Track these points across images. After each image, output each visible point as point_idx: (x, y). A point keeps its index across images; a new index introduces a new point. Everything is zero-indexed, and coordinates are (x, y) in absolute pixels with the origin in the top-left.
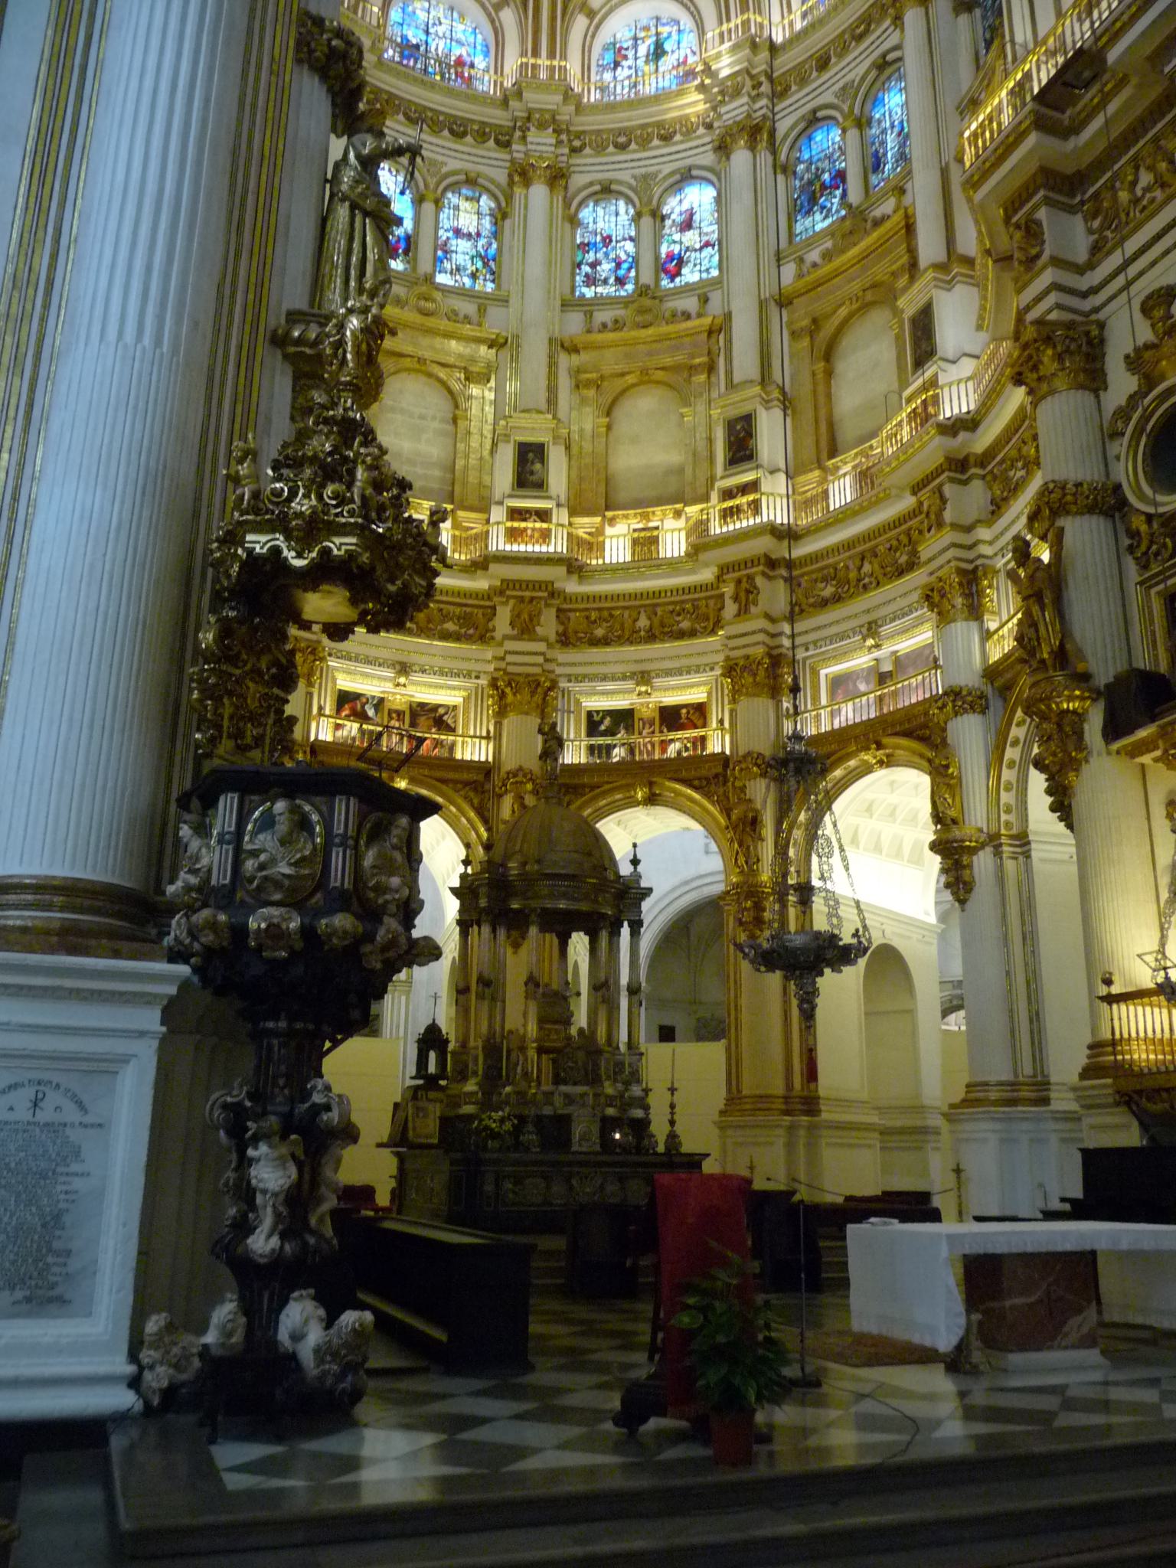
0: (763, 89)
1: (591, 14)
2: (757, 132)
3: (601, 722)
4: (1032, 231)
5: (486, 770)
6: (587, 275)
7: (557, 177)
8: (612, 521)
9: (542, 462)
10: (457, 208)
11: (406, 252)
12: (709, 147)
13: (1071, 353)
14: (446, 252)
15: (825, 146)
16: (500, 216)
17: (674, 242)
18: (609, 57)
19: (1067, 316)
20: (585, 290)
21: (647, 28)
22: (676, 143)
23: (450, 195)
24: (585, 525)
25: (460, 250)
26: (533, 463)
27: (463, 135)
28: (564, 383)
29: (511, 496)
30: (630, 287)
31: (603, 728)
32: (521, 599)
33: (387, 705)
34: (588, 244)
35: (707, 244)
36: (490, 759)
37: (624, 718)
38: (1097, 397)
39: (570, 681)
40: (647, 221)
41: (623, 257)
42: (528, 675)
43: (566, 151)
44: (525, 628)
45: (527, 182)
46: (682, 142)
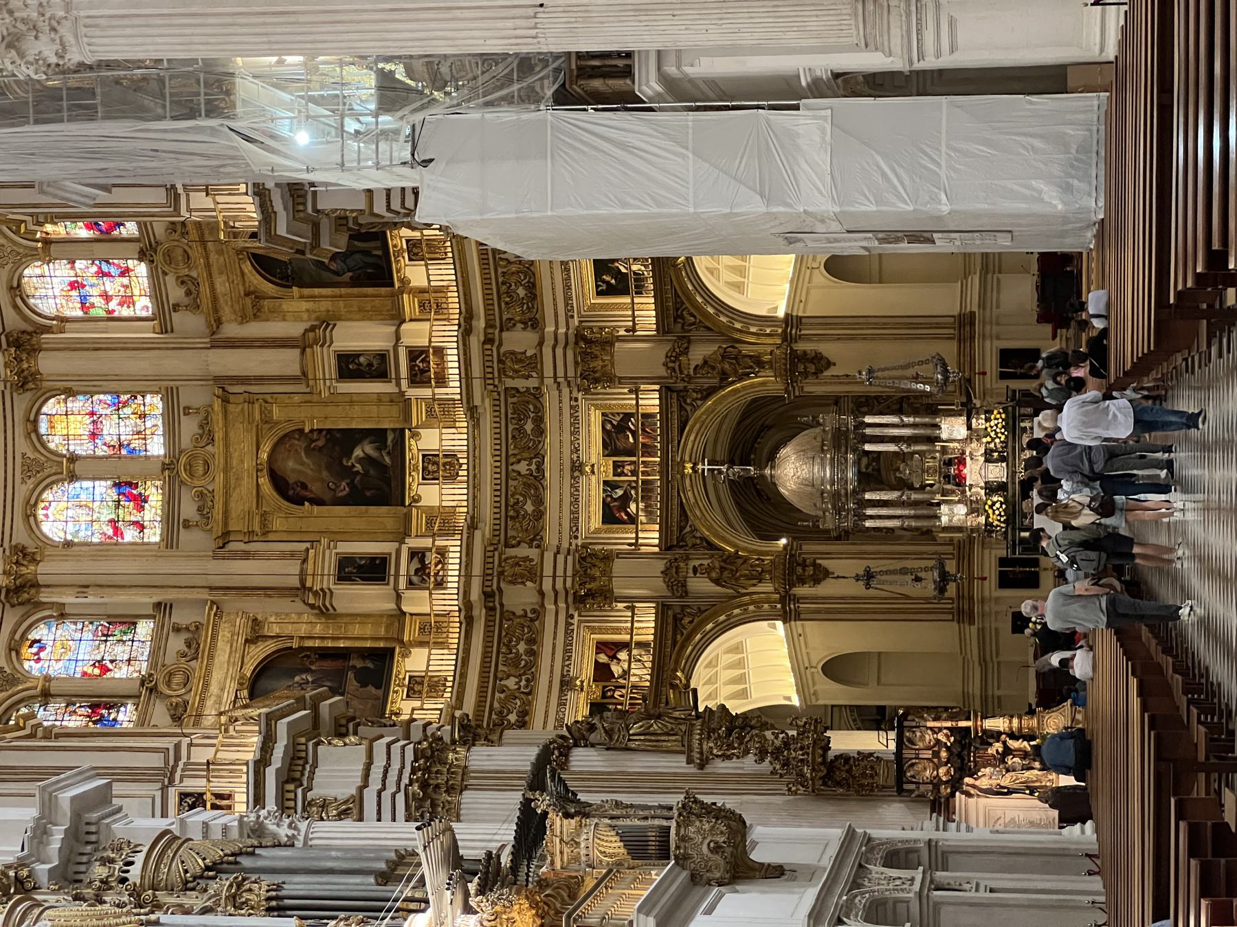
3: (608, 283)
5: (666, 392)
6: (121, 304)
8: (405, 282)
9: (359, 355)
16: (70, 393)
20: (138, 306)
23: (52, 446)
24: (409, 304)
25: (114, 431)
26: (360, 364)
28: (255, 329)
29: (398, 384)
30: (131, 263)
31: (613, 281)
32: (502, 372)
33: (611, 478)
36: (657, 387)
39: (572, 317)
41: (95, 269)
42: (576, 363)
44: (532, 364)
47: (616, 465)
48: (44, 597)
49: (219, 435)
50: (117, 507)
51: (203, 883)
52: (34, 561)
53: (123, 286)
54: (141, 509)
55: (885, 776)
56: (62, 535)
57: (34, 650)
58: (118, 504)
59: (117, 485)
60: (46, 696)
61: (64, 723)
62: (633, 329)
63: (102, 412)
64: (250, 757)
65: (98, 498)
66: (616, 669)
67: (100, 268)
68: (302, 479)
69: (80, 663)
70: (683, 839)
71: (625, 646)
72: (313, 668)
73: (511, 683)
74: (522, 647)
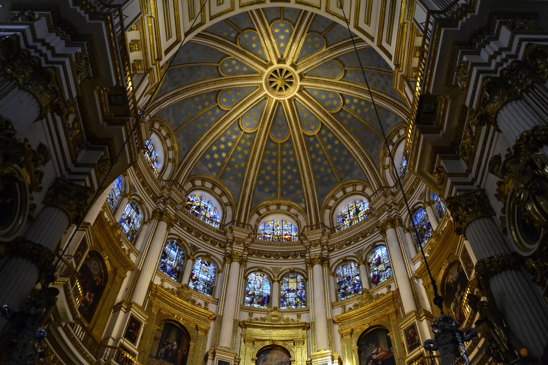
0: (393, 208)
1: (330, 208)
2: (393, 222)
4: (440, 170)
6: (343, 293)
7: (323, 261)
12: (379, 234)
13: (471, 206)
15: (421, 217)
16: (305, 281)
17: (375, 271)
18: (340, 219)
19: (462, 193)
20: (342, 299)
21: (352, 206)
22: (368, 237)
27: (288, 257)
28: (338, 336)
34: (342, 281)
35: (388, 267)
38: (492, 219)
40: (362, 267)
41: (356, 282)
43: (327, 251)
46: (370, 236)
48: (227, 265)
50: (259, 296)
53: (350, 292)
54: (258, 303)
56: (250, 279)
57: (206, 263)
58: (262, 296)
60: (186, 257)
61: (174, 261)
63: (298, 292)
65: (263, 291)
67: (357, 284)
68: (268, 360)
69: (198, 274)
72: (179, 351)
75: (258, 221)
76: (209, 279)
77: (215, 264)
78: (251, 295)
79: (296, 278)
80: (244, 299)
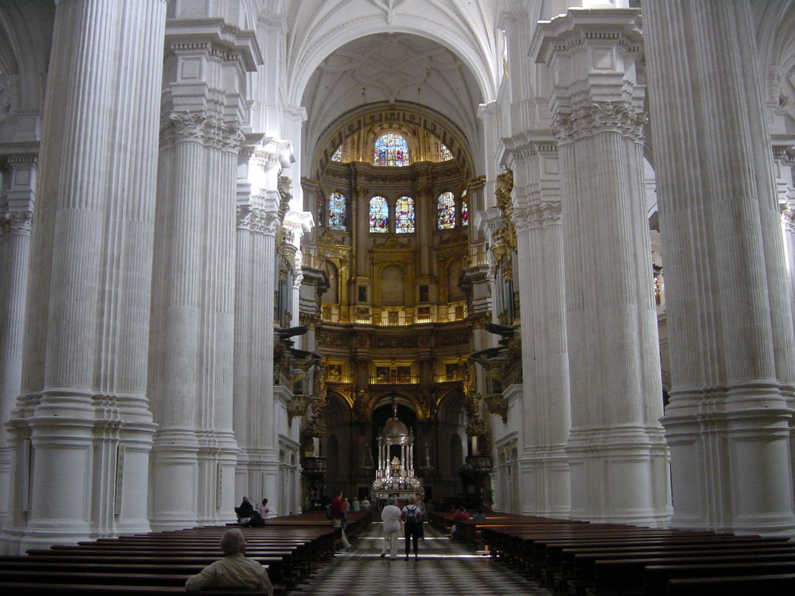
8: (449, 306)
10: (401, 204)
11: (386, 225)
14: (399, 221)
16: (414, 206)
20: (441, 226)
23: (399, 200)
25: (403, 219)
28: (435, 261)
30: (454, 224)
34: (441, 209)
37: (456, 366)
41: (452, 213)
45: (420, 196)
47: (393, 371)
49: (403, 250)
51: (284, 261)
52: (364, 196)
54: (380, 226)
55: (308, 454)
58: (381, 220)
59: (387, 219)
62: (436, 375)
64: (312, 266)
66: (333, 371)
70: (299, 398)
71: (340, 374)
73: (328, 339)
74: (339, 342)
75: (374, 141)
76: (342, 212)
77: (344, 194)
78: (373, 219)
79: (407, 200)
80: (369, 224)
